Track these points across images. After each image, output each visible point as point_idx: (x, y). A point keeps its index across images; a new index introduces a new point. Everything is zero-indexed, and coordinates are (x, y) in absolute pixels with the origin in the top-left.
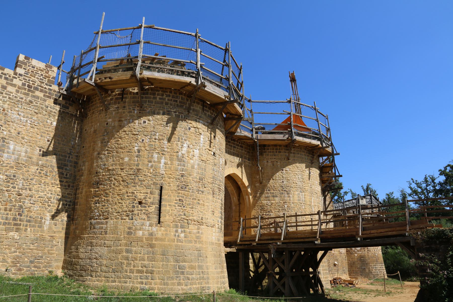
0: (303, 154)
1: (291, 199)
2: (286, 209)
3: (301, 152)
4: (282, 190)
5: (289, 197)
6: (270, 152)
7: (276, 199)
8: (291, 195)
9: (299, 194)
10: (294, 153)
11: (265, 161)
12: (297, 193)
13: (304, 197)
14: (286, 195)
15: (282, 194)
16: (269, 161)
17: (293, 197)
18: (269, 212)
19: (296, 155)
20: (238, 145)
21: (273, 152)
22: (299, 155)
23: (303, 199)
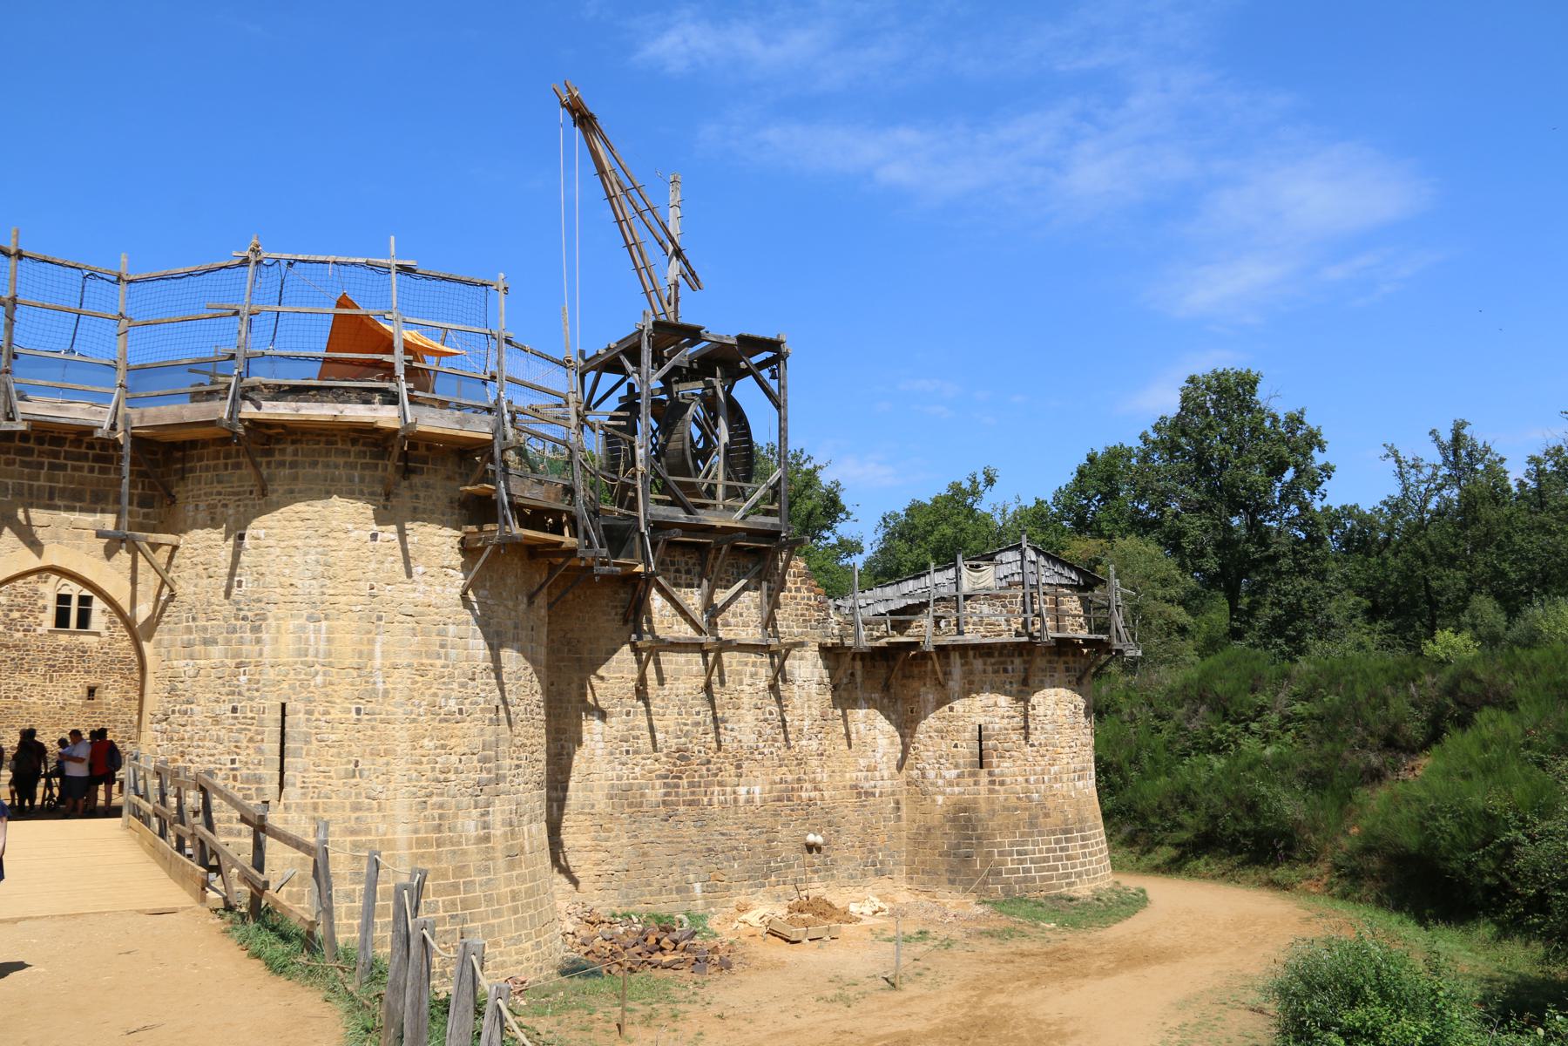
0: (341, 460)
1: (267, 649)
2: (243, 689)
3: (328, 454)
4: (237, 619)
5: (258, 641)
6: (207, 469)
7: (216, 651)
8: (264, 636)
9: (303, 628)
10: (293, 465)
11: (191, 507)
12: (291, 624)
13: (329, 641)
14: (248, 635)
15: (234, 631)
16: (202, 506)
17: (276, 640)
18: (189, 702)
19: (301, 471)
20: (85, 457)
21: (216, 468)
22: (319, 470)
23: (322, 646)
